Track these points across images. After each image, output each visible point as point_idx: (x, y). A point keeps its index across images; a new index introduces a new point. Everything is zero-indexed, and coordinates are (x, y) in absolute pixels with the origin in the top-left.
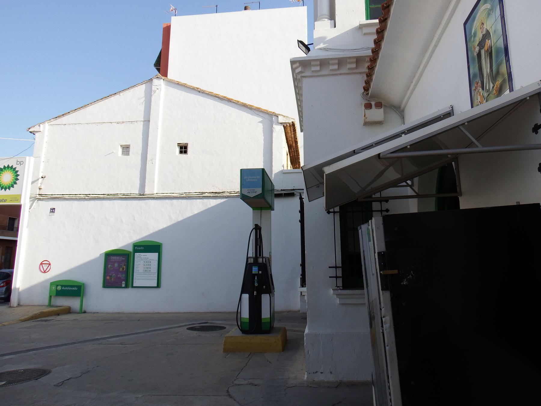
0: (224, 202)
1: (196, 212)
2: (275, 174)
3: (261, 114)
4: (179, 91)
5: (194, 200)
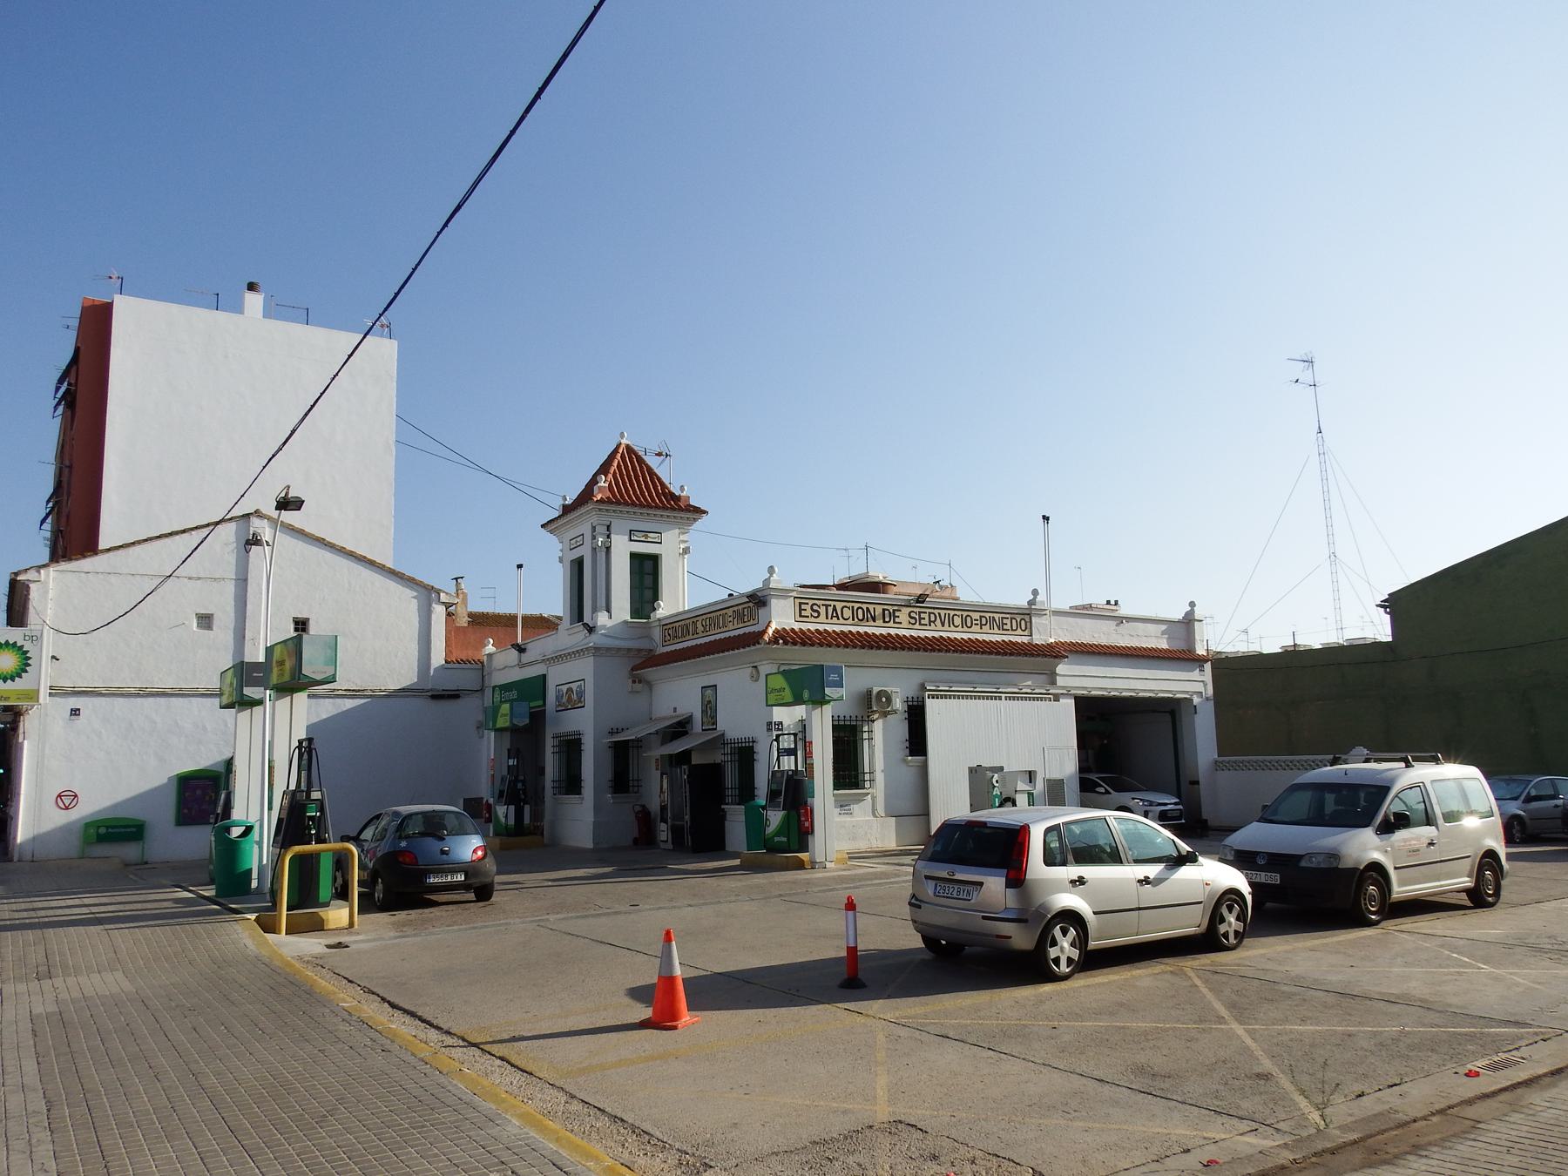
0: (365, 703)
1: (325, 717)
2: (435, 669)
3: (415, 586)
4: (292, 539)
5: (322, 700)
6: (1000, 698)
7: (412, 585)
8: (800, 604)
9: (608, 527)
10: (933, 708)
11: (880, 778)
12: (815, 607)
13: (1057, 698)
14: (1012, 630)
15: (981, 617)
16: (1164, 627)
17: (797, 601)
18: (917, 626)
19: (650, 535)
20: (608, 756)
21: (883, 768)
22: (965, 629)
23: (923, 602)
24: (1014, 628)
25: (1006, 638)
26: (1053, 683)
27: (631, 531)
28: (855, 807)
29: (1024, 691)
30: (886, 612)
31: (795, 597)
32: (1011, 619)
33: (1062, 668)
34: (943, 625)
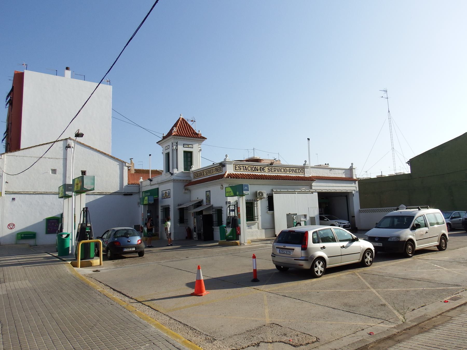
1: (91, 201)
3: (118, 161)
4: (80, 146)
5: (90, 196)
6: (295, 193)
7: (117, 160)
8: (235, 166)
9: (177, 143)
10: (275, 197)
11: (260, 218)
12: (240, 167)
13: (312, 193)
14: (299, 173)
15: (289, 169)
16: (344, 171)
17: (234, 165)
18: (270, 172)
19: (189, 145)
20: (178, 212)
21: (260, 215)
22: (285, 173)
23: (272, 165)
24: (299, 172)
25: (297, 175)
26: (311, 188)
27: (184, 144)
28: (253, 227)
29: (302, 191)
30: (261, 168)
31: (234, 164)
32: (299, 169)
33: (314, 184)
34: (278, 172)
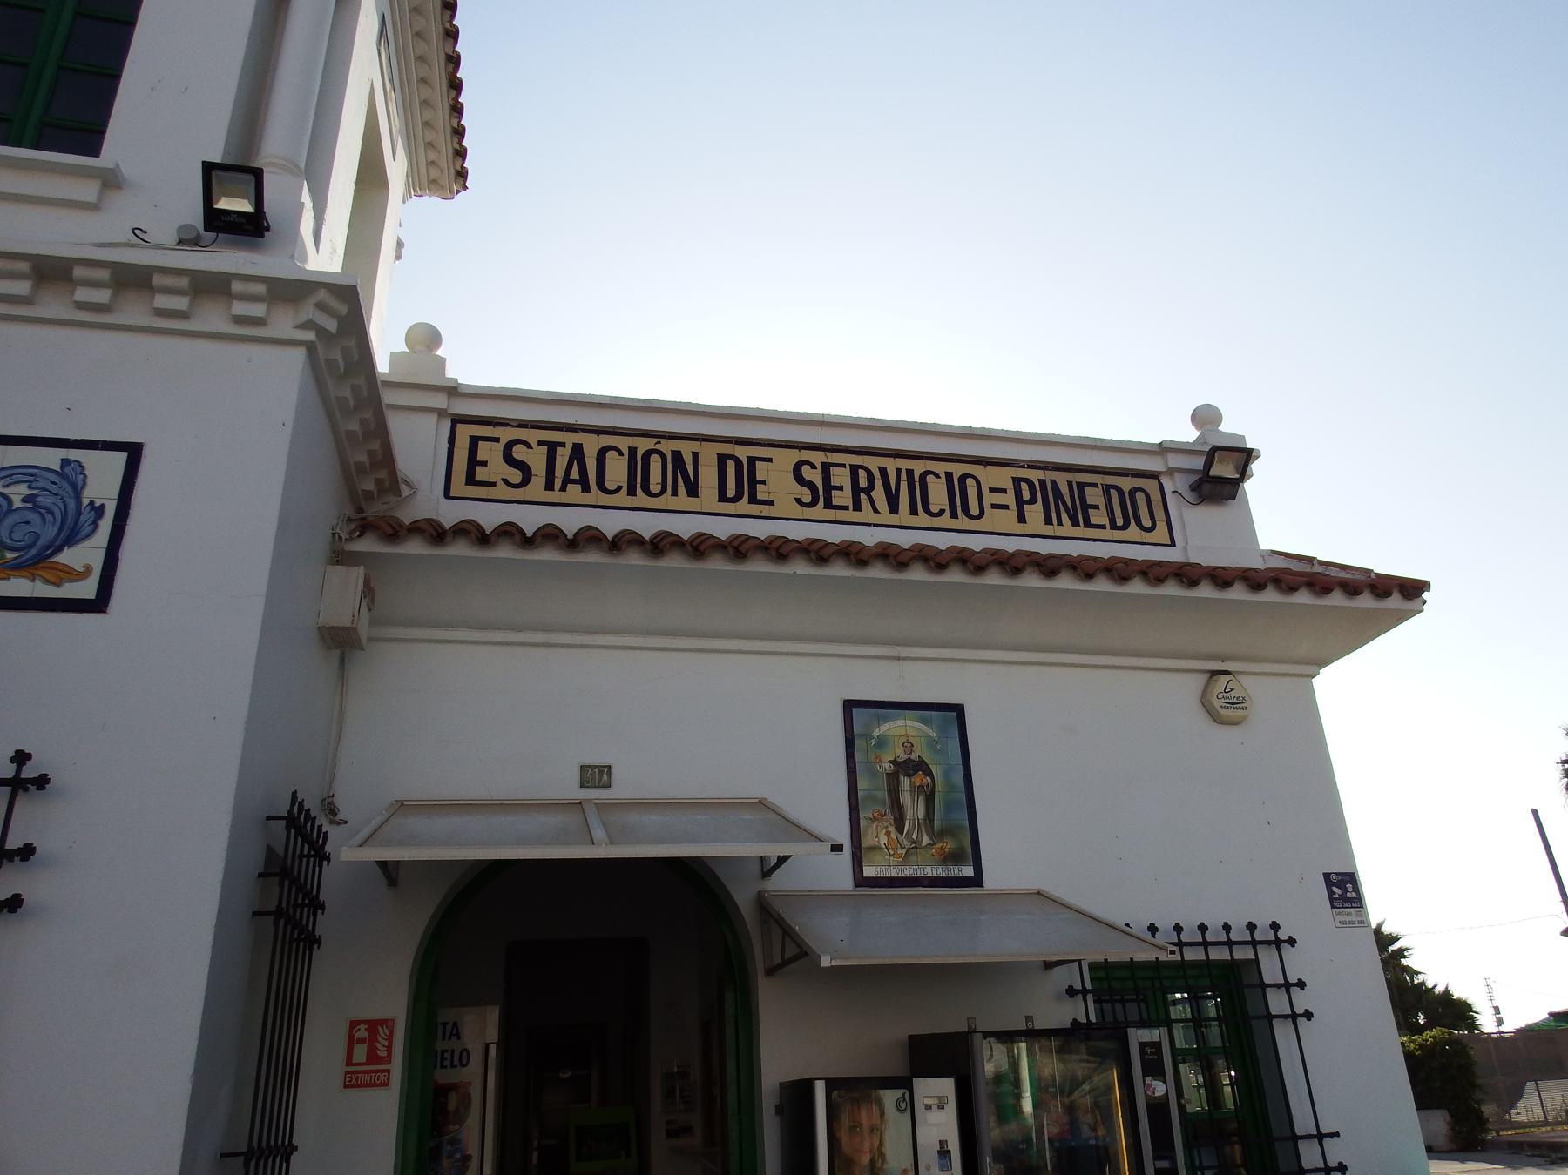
8: (474, 441)
15: (1017, 481)
34: (894, 509)
